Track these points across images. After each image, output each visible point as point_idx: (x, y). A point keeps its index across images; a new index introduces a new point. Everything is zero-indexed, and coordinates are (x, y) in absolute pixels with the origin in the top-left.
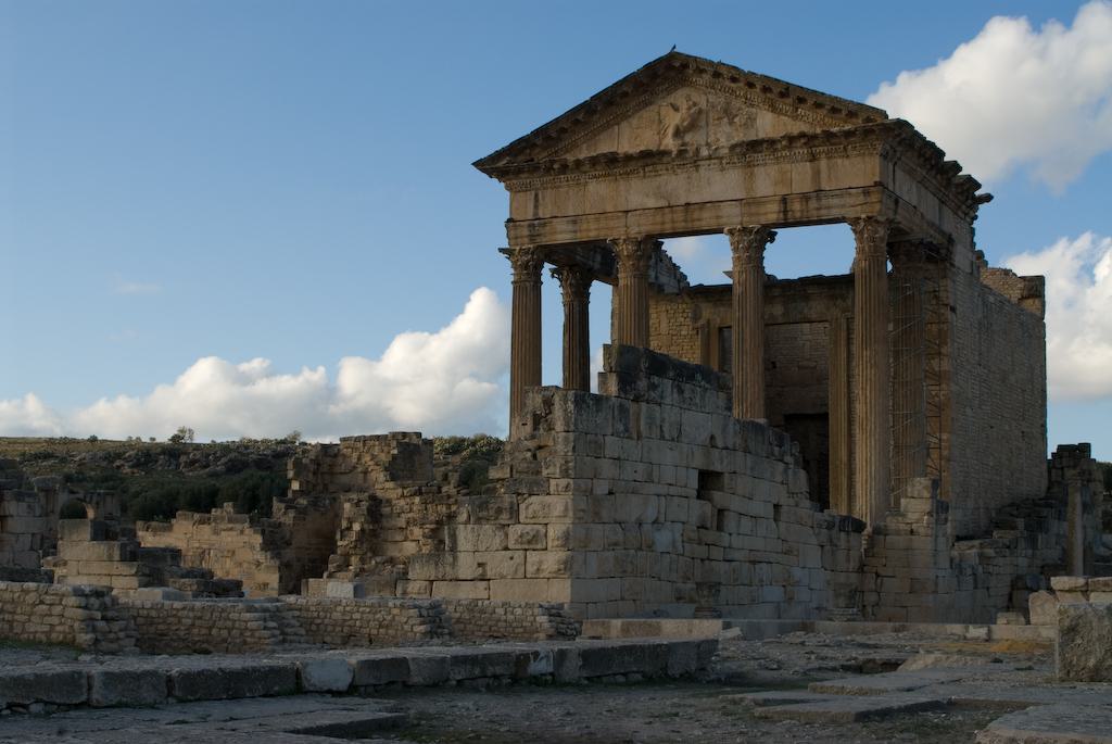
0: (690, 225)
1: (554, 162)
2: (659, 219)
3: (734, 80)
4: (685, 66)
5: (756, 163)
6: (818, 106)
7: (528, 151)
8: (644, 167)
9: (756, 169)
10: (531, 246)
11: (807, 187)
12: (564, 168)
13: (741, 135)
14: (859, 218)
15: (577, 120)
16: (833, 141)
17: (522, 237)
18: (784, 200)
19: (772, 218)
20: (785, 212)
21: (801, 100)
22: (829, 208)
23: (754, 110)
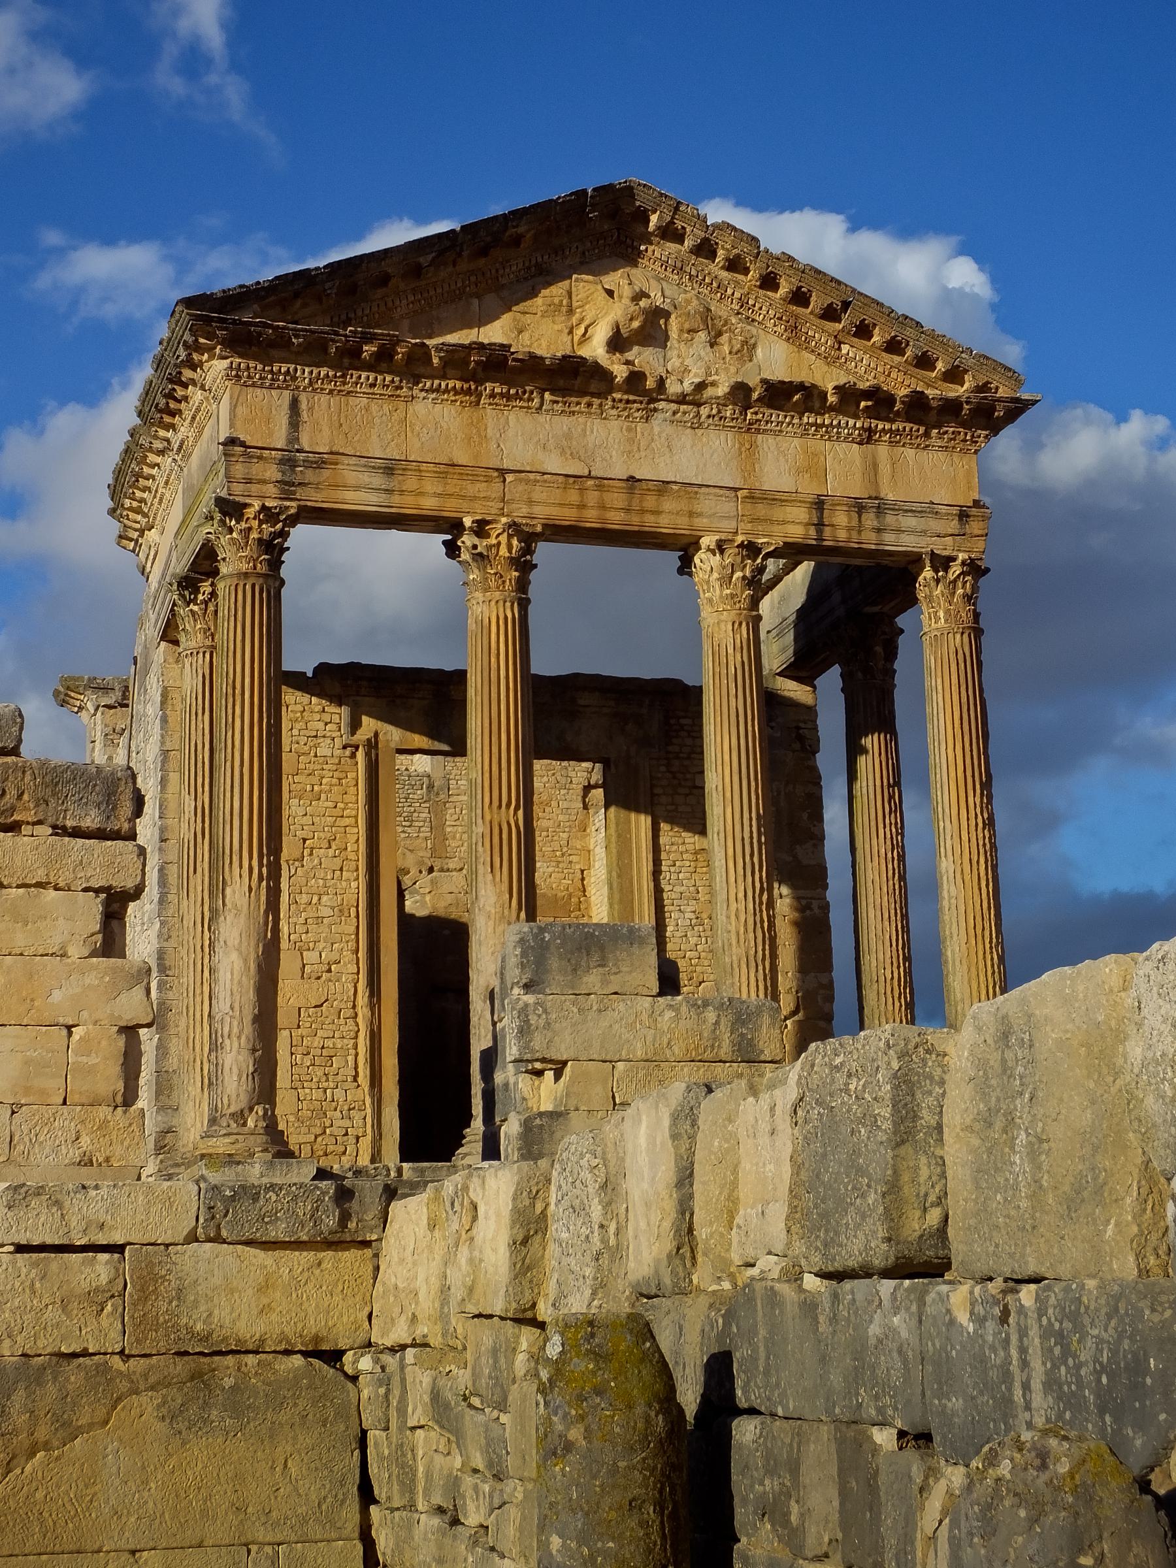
0: (635, 519)
2: (573, 496)
6: (893, 347)
7: (299, 303)
10: (294, 504)
13: (733, 369)
17: (263, 482)
18: (819, 504)
20: (820, 525)
22: (899, 531)
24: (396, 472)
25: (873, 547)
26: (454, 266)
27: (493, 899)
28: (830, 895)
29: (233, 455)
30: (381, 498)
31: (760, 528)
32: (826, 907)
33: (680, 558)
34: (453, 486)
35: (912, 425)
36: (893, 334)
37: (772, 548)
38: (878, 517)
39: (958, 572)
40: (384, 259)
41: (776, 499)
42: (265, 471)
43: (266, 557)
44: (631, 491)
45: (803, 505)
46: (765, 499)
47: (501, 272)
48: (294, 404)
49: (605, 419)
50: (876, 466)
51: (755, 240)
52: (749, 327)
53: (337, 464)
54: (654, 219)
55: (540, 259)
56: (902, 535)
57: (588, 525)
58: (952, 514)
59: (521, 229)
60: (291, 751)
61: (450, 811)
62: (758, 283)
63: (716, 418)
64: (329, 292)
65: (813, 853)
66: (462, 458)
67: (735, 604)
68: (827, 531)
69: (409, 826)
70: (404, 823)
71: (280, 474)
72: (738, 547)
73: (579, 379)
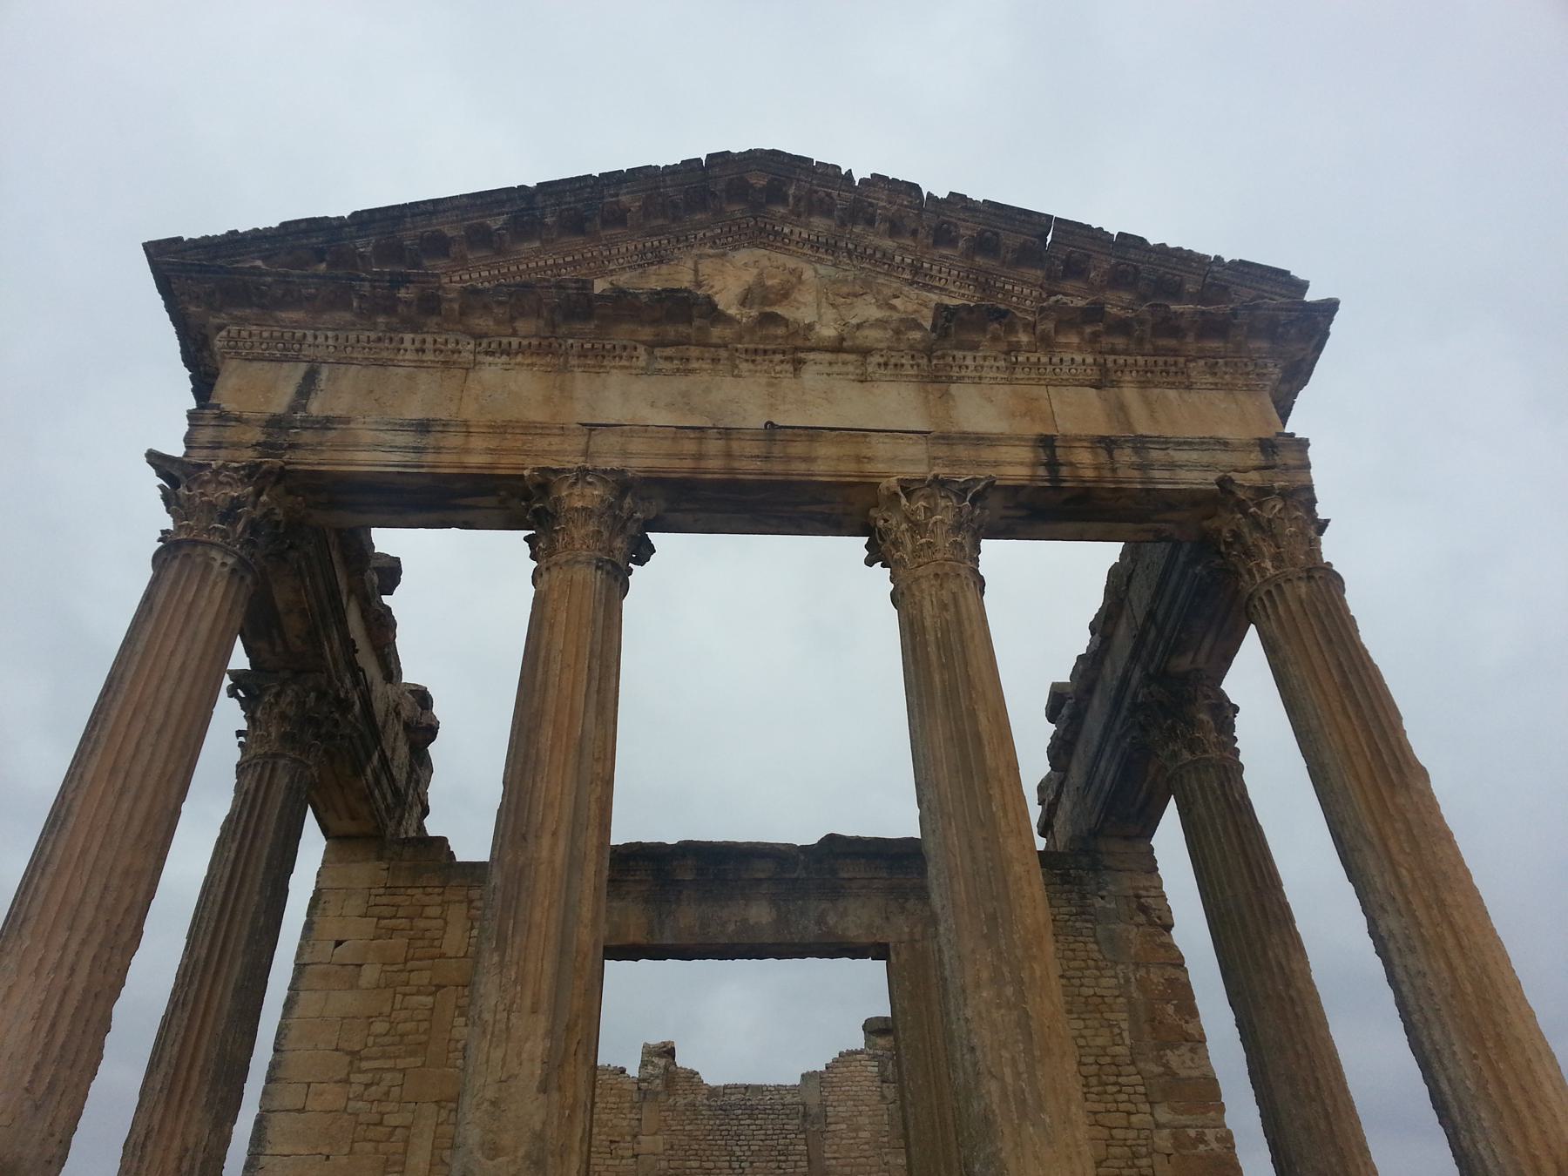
0: (778, 467)
1: (399, 281)
2: (689, 446)
3: (895, 230)
4: (775, 193)
5: (955, 373)
7: (323, 266)
8: (651, 346)
9: (954, 388)
12: (430, 304)
15: (489, 227)
16: (1162, 342)
17: (236, 445)
18: (1046, 443)
20: (1052, 465)
21: (1074, 269)
25: (1139, 486)
28: (1231, 1120)
29: (202, 419)
30: (411, 457)
32: (1227, 1140)
35: (1164, 358)
37: (983, 483)
38: (1136, 453)
40: (432, 213)
41: (983, 438)
42: (244, 434)
46: (966, 438)
48: (310, 379)
49: (740, 376)
50: (1122, 407)
51: (915, 188)
53: (349, 423)
54: (791, 191)
55: (656, 243)
56: (1178, 471)
57: (709, 476)
59: (623, 198)
60: (465, 956)
62: (931, 241)
63: (891, 367)
65: (1192, 1060)
66: (536, 415)
68: (1064, 472)
69: (784, 1161)
70: (779, 1158)
72: (929, 486)
73: (697, 322)
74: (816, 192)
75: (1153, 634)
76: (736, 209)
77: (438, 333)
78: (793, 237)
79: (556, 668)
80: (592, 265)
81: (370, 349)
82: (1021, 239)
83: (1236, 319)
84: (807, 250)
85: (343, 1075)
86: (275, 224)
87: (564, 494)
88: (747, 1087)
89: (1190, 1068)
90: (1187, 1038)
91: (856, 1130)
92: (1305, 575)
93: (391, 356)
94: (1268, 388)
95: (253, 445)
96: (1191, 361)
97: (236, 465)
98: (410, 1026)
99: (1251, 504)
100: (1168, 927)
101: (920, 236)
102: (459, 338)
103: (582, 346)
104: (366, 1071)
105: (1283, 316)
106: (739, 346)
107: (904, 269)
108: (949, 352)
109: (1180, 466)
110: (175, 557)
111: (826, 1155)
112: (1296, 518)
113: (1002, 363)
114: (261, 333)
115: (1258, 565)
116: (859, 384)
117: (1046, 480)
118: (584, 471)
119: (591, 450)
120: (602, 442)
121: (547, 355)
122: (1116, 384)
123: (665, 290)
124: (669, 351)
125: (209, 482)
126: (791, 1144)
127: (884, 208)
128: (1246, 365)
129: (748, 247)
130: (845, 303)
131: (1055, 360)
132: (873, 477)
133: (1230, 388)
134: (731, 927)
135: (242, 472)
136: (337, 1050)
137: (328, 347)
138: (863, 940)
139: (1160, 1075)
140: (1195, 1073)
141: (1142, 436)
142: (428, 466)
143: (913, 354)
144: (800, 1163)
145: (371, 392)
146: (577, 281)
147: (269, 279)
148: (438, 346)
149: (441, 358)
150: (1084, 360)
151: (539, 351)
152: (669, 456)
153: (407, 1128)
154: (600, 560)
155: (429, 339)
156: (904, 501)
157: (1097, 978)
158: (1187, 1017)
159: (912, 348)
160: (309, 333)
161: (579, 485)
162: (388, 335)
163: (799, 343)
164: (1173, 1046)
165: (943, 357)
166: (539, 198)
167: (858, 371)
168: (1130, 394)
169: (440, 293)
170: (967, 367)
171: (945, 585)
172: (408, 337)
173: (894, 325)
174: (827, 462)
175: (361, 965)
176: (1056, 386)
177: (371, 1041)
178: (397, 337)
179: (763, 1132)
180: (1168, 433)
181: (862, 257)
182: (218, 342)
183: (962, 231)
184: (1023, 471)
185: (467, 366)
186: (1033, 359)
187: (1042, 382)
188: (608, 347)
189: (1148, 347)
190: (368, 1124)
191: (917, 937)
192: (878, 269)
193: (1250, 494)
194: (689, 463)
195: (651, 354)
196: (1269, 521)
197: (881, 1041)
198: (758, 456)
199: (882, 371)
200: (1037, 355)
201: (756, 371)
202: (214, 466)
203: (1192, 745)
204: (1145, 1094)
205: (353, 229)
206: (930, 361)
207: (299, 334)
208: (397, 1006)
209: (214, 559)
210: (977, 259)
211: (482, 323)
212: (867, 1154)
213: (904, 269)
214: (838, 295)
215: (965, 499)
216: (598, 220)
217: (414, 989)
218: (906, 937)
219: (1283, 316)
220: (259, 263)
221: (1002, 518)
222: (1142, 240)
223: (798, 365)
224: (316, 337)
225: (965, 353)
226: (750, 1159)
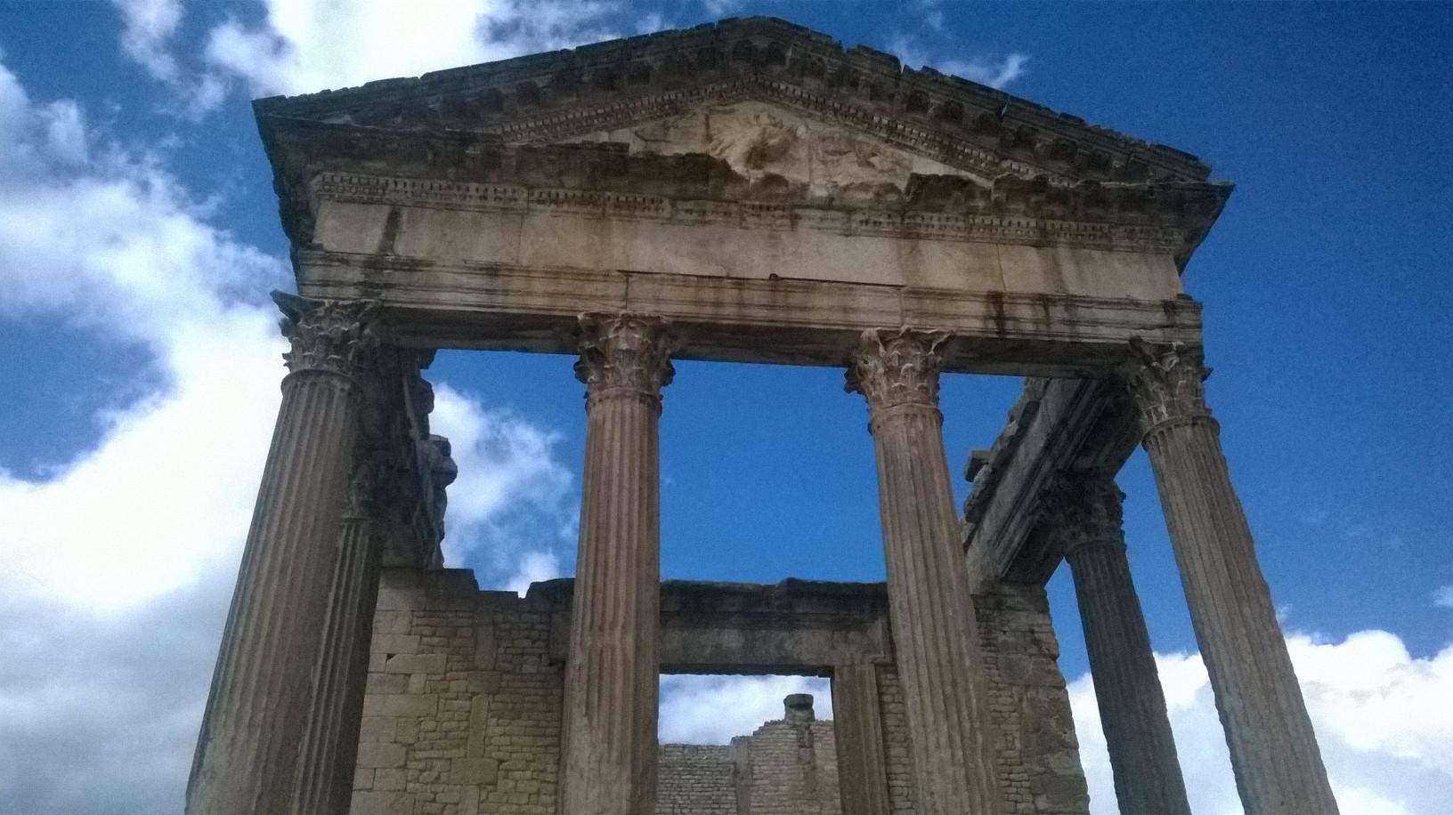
0: (781, 315)
1: (466, 140)
2: (708, 295)
3: (875, 93)
4: (775, 55)
5: (923, 231)
6: (1060, 151)
7: (399, 120)
8: (674, 200)
11: (1038, 285)
12: (492, 161)
14: (1169, 348)
16: (1094, 211)
17: (341, 284)
18: (996, 298)
19: (973, 326)
20: (1000, 318)
21: (1023, 140)
23: (905, 154)
24: (499, 273)
25: (1067, 340)
26: (578, 96)
27: (587, 751)
29: (310, 259)
31: (930, 323)
33: (846, 375)
34: (564, 286)
35: (1092, 224)
36: (1056, 136)
37: (945, 336)
39: (1175, 362)
41: (946, 294)
42: (346, 273)
43: (333, 356)
44: (774, 290)
45: (978, 299)
47: (631, 105)
48: (393, 222)
49: (746, 228)
50: (1056, 266)
52: (898, 152)
54: (789, 54)
55: (673, 97)
58: (1154, 306)
59: (648, 59)
60: (494, 669)
61: (755, 794)
62: (905, 106)
64: (431, 106)
66: (583, 261)
67: (905, 396)
68: (1009, 325)
71: (363, 276)
72: (903, 337)
73: (712, 183)
74: (810, 56)
75: (1064, 436)
76: (741, 67)
77: (498, 183)
78: (788, 94)
79: (615, 488)
80: (619, 116)
81: (442, 195)
82: (981, 111)
83: (1152, 195)
84: (799, 105)
85: (402, 763)
86: (360, 84)
87: (611, 336)
88: (684, 747)
89: (1065, 768)
90: (1063, 744)
91: (778, 784)
92: (1191, 422)
93: (459, 202)
94: (1173, 252)
95: (355, 284)
96: (1112, 227)
97: (346, 303)
98: (454, 724)
99: (1153, 357)
100: (1054, 658)
101: (895, 101)
102: (516, 188)
103: (618, 199)
104: (420, 760)
105: (1188, 194)
106: (748, 202)
107: (881, 128)
108: (920, 213)
109: (1102, 323)
110: (303, 385)
111: (752, 804)
112: (1188, 371)
113: (961, 224)
114: (351, 180)
115: (1156, 409)
116: (845, 239)
117: (997, 333)
118: (627, 319)
119: (629, 297)
120: (640, 289)
121: (589, 204)
122: (1054, 245)
123: (688, 155)
124: (689, 205)
125: (324, 317)
126: (723, 795)
127: (865, 75)
128: (1157, 232)
129: (749, 100)
130: (833, 161)
131: (1005, 223)
132: (857, 326)
133: (1143, 251)
134: (708, 651)
135: (349, 310)
136: (395, 742)
137: (406, 192)
138: (814, 663)
139: (1041, 774)
140: (1068, 772)
141: (1073, 296)
142: (500, 307)
143: (890, 211)
144: (731, 811)
145: (445, 235)
146: (616, 144)
147: (358, 135)
148: (499, 195)
149: (501, 204)
150: (1028, 224)
151: (582, 202)
152: (696, 303)
153: (456, 804)
154: (642, 395)
155: (491, 189)
156: (881, 350)
157: (997, 697)
158: (1066, 730)
159: (888, 208)
160: (391, 180)
161: (624, 329)
162: (457, 183)
163: (798, 201)
164: (1051, 750)
165: (914, 217)
166: (578, 59)
167: (844, 227)
168: (1063, 253)
169: (501, 150)
170: (933, 226)
171: (913, 424)
172: (473, 186)
173: (875, 189)
174: (822, 312)
175: (409, 675)
176: (1004, 244)
177: (422, 735)
178: (464, 185)
179: (700, 785)
180: (1093, 294)
181: (846, 115)
182: (315, 184)
183: (932, 101)
184: (975, 325)
185: (521, 212)
186: (987, 222)
187: (994, 241)
188: (640, 200)
189: (1080, 214)
190: (425, 801)
191: (857, 662)
192: (859, 126)
193: (1154, 350)
194: (708, 310)
195: (673, 205)
196: (1167, 373)
197: (800, 714)
198: (764, 305)
199: (864, 227)
200: (991, 217)
201: (760, 225)
202: (327, 305)
203: (1091, 528)
204: (1030, 788)
205: (424, 88)
206: (903, 219)
207: (382, 181)
208: (441, 707)
209: (335, 387)
210: (946, 126)
211: (536, 177)
212: (787, 804)
213: (881, 128)
214: (826, 152)
215: (931, 346)
216: (625, 78)
217: (455, 695)
218: (848, 662)
219: (1188, 194)
220: (347, 118)
221: (957, 358)
222: (1081, 121)
223: (795, 219)
224: (396, 183)
225: (931, 214)
226: (689, 807)
